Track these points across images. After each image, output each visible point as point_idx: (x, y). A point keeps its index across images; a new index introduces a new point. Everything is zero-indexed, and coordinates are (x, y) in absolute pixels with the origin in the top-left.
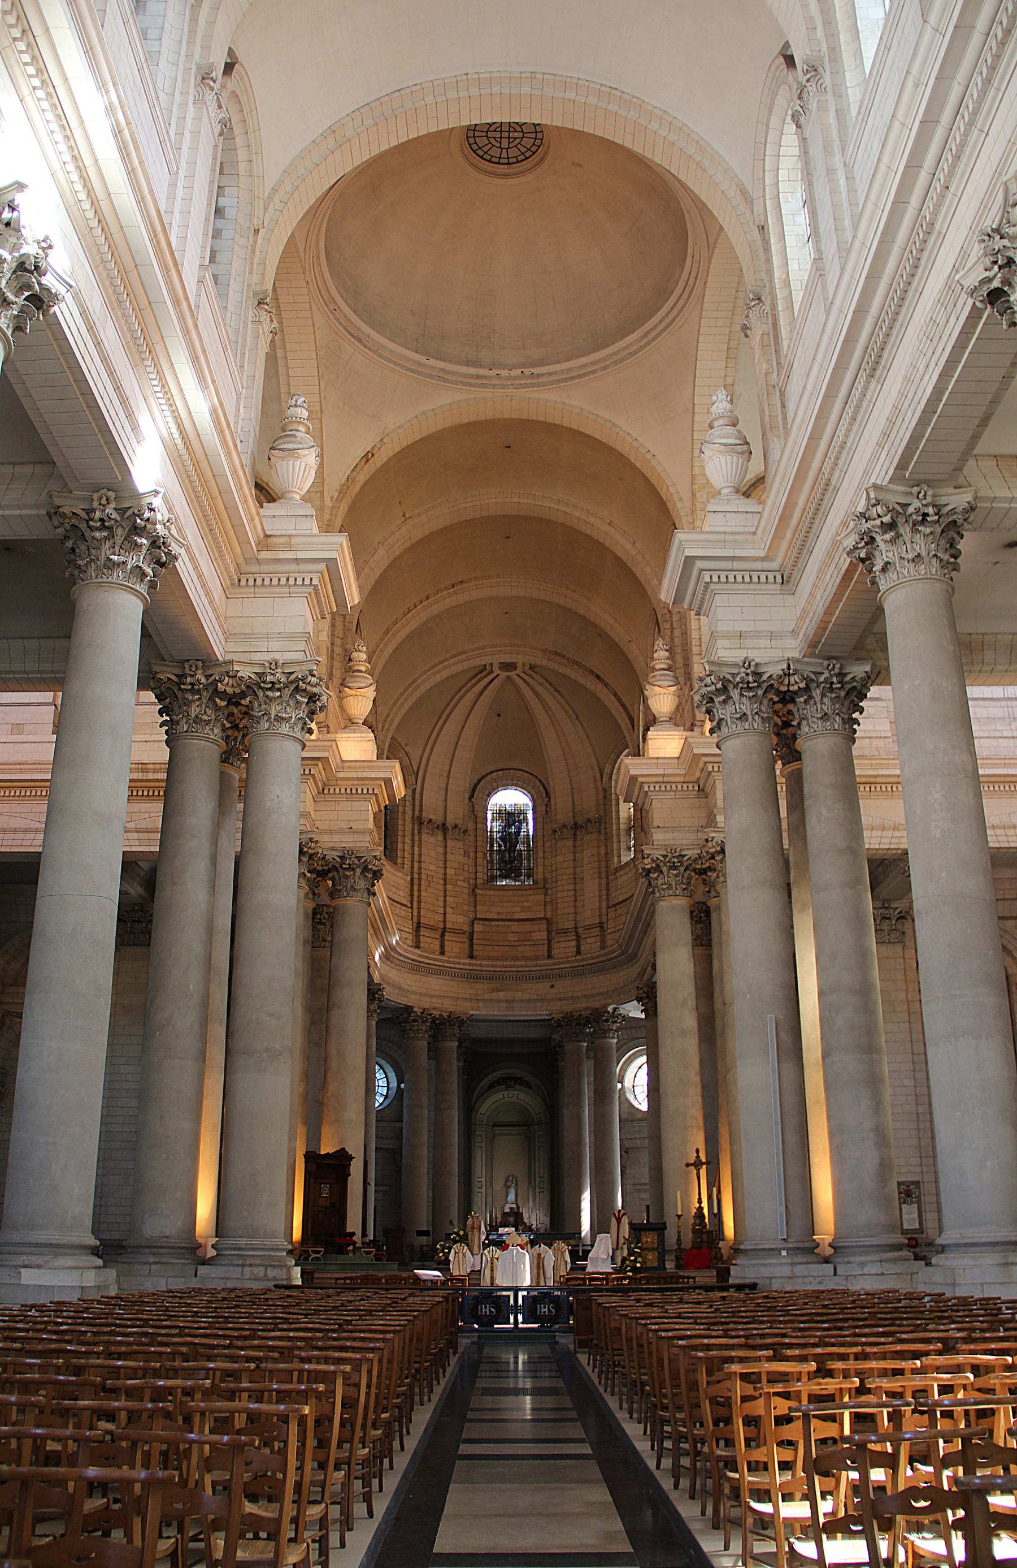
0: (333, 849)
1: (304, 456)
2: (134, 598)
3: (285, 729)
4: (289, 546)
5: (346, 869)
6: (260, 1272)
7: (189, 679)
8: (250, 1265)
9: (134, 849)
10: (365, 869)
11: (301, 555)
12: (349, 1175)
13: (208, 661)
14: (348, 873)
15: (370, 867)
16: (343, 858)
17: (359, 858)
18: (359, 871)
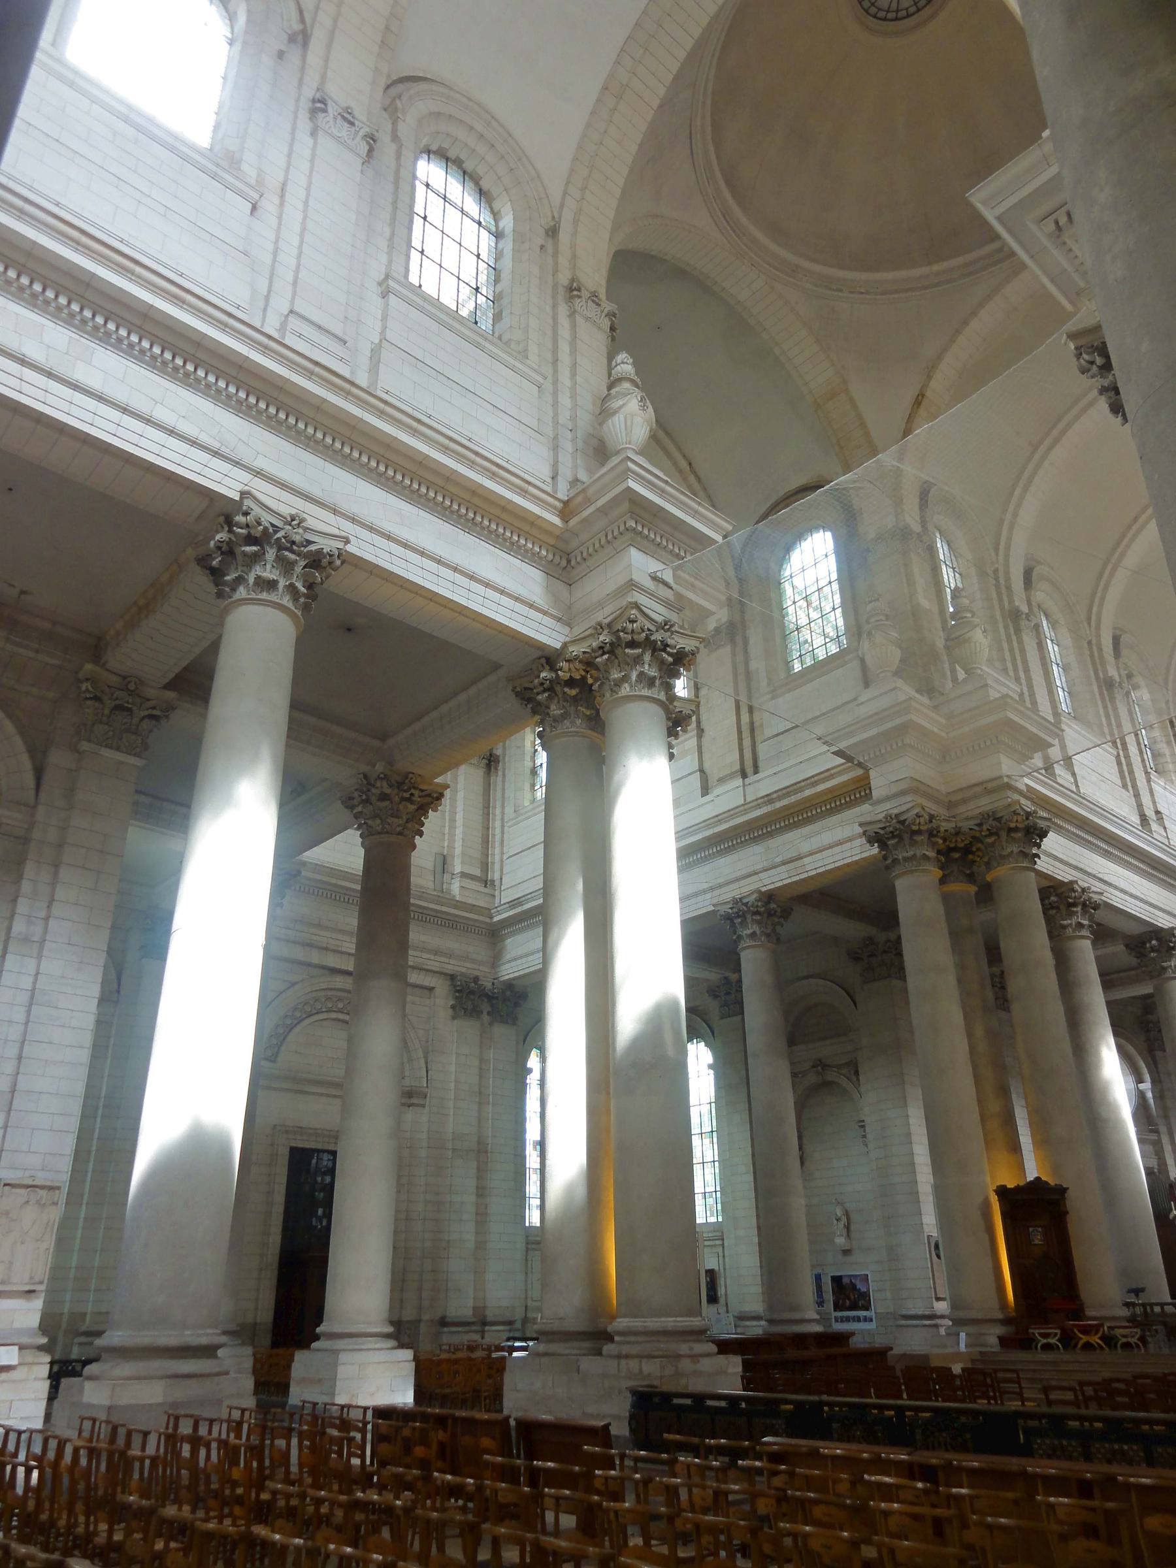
0: (968, 819)
1: (621, 407)
2: (256, 607)
3: (626, 689)
4: (589, 501)
5: (986, 836)
6: (634, 1364)
7: (536, 681)
8: (627, 1357)
9: (785, 882)
10: (1010, 830)
11: (600, 503)
12: (1067, 1213)
13: (549, 658)
14: (990, 840)
15: (1013, 825)
16: (980, 825)
17: (999, 820)
18: (1003, 834)
